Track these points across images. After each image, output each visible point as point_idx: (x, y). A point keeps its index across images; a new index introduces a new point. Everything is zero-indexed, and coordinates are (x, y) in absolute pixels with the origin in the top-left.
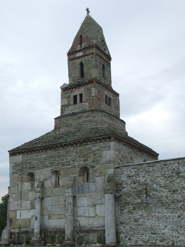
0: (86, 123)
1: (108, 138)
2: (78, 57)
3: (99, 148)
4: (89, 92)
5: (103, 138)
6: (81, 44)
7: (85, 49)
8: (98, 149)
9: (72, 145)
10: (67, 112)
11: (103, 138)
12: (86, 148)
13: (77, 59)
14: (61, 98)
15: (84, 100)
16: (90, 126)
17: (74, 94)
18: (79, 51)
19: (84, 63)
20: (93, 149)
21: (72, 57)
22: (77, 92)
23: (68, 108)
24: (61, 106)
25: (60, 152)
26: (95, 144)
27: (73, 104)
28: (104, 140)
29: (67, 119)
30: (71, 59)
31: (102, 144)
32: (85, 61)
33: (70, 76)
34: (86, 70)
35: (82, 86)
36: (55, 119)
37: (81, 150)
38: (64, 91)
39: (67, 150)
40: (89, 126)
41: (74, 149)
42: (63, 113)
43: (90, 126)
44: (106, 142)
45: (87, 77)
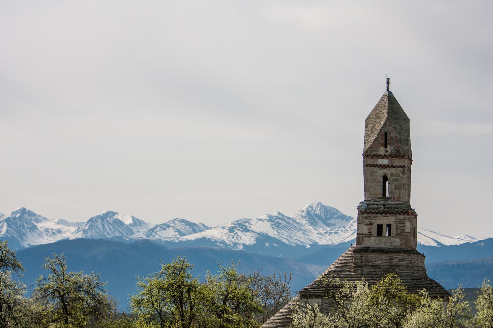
0: (401, 268)
4: (401, 225)
6: (386, 147)
7: (393, 157)
13: (379, 167)
15: (393, 233)
17: (379, 222)
18: (383, 157)
21: (370, 161)
22: (384, 220)
30: (369, 165)
32: (392, 175)
33: (366, 189)
34: (393, 187)
35: (391, 214)
42: (361, 244)
45: (394, 199)
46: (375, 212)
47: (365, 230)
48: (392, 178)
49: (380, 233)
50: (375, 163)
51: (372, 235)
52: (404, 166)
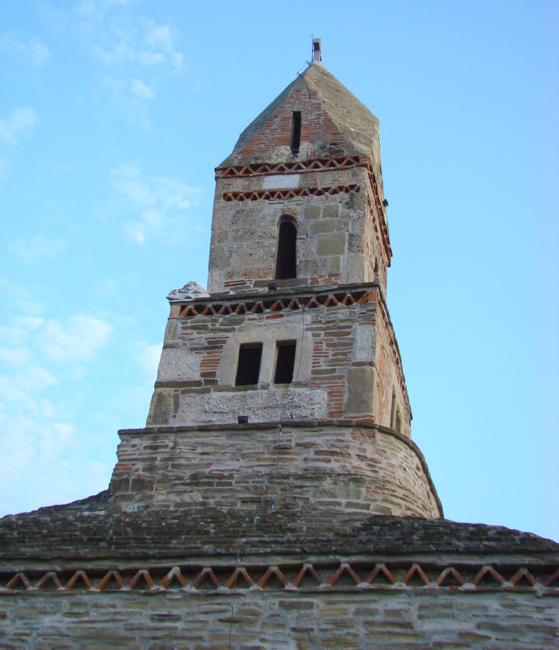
0: (327, 484)
1: (534, 570)
2: (272, 193)
3: (469, 626)
4: (335, 340)
5: (508, 571)
6: (295, 146)
7: (316, 166)
8: (461, 634)
9: (273, 581)
10: (191, 413)
11: (508, 571)
12: (372, 612)
13: (267, 198)
14: (165, 347)
15: (302, 368)
16: (349, 505)
19: (300, 218)
20: (428, 626)
21: (239, 185)
22: (266, 332)
23: (198, 398)
24: (158, 385)
25: (175, 612)
26: (443, 599)
27: (233, 383)
28: (507, 584)
29: (204, 444)
30: (235, 195)
31: (493, 603)
32: (310, 213)
34: (314, 249)
35: (295, 307)
36: (122, 433)
37: (340, 624)
38: (190, 314)
39: (234, 607)
40: (344, 501)
41: (282, 604)
43: (349, 505)
44: (521, 599)
46: (234, 308)
47: (190, 367)
48: (312, 222)
49: (248, 374)
50: (255, 188)
51: (214, 382)
52: (352, 187)
